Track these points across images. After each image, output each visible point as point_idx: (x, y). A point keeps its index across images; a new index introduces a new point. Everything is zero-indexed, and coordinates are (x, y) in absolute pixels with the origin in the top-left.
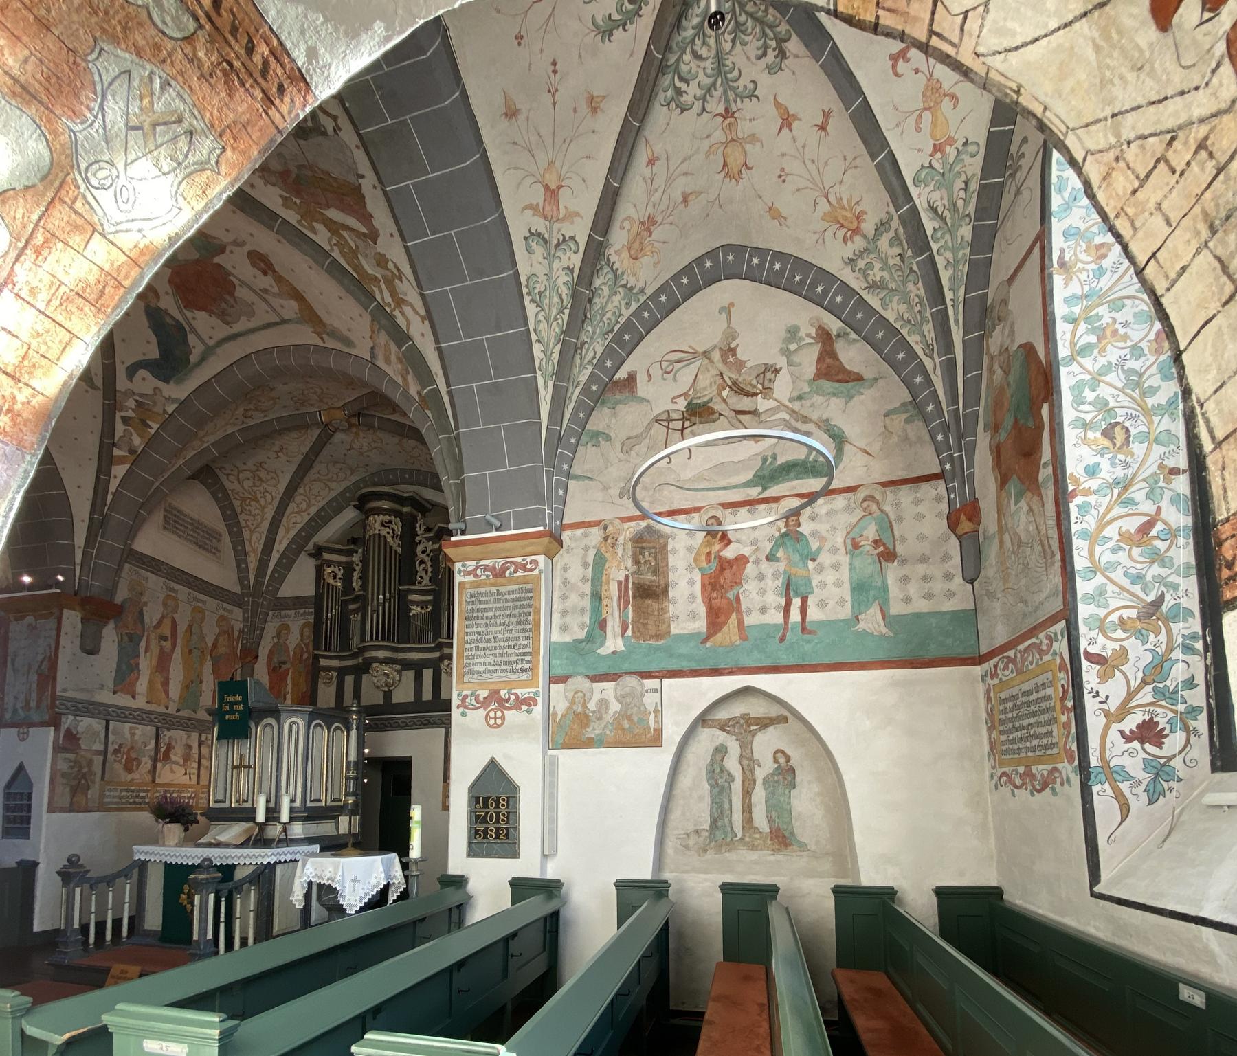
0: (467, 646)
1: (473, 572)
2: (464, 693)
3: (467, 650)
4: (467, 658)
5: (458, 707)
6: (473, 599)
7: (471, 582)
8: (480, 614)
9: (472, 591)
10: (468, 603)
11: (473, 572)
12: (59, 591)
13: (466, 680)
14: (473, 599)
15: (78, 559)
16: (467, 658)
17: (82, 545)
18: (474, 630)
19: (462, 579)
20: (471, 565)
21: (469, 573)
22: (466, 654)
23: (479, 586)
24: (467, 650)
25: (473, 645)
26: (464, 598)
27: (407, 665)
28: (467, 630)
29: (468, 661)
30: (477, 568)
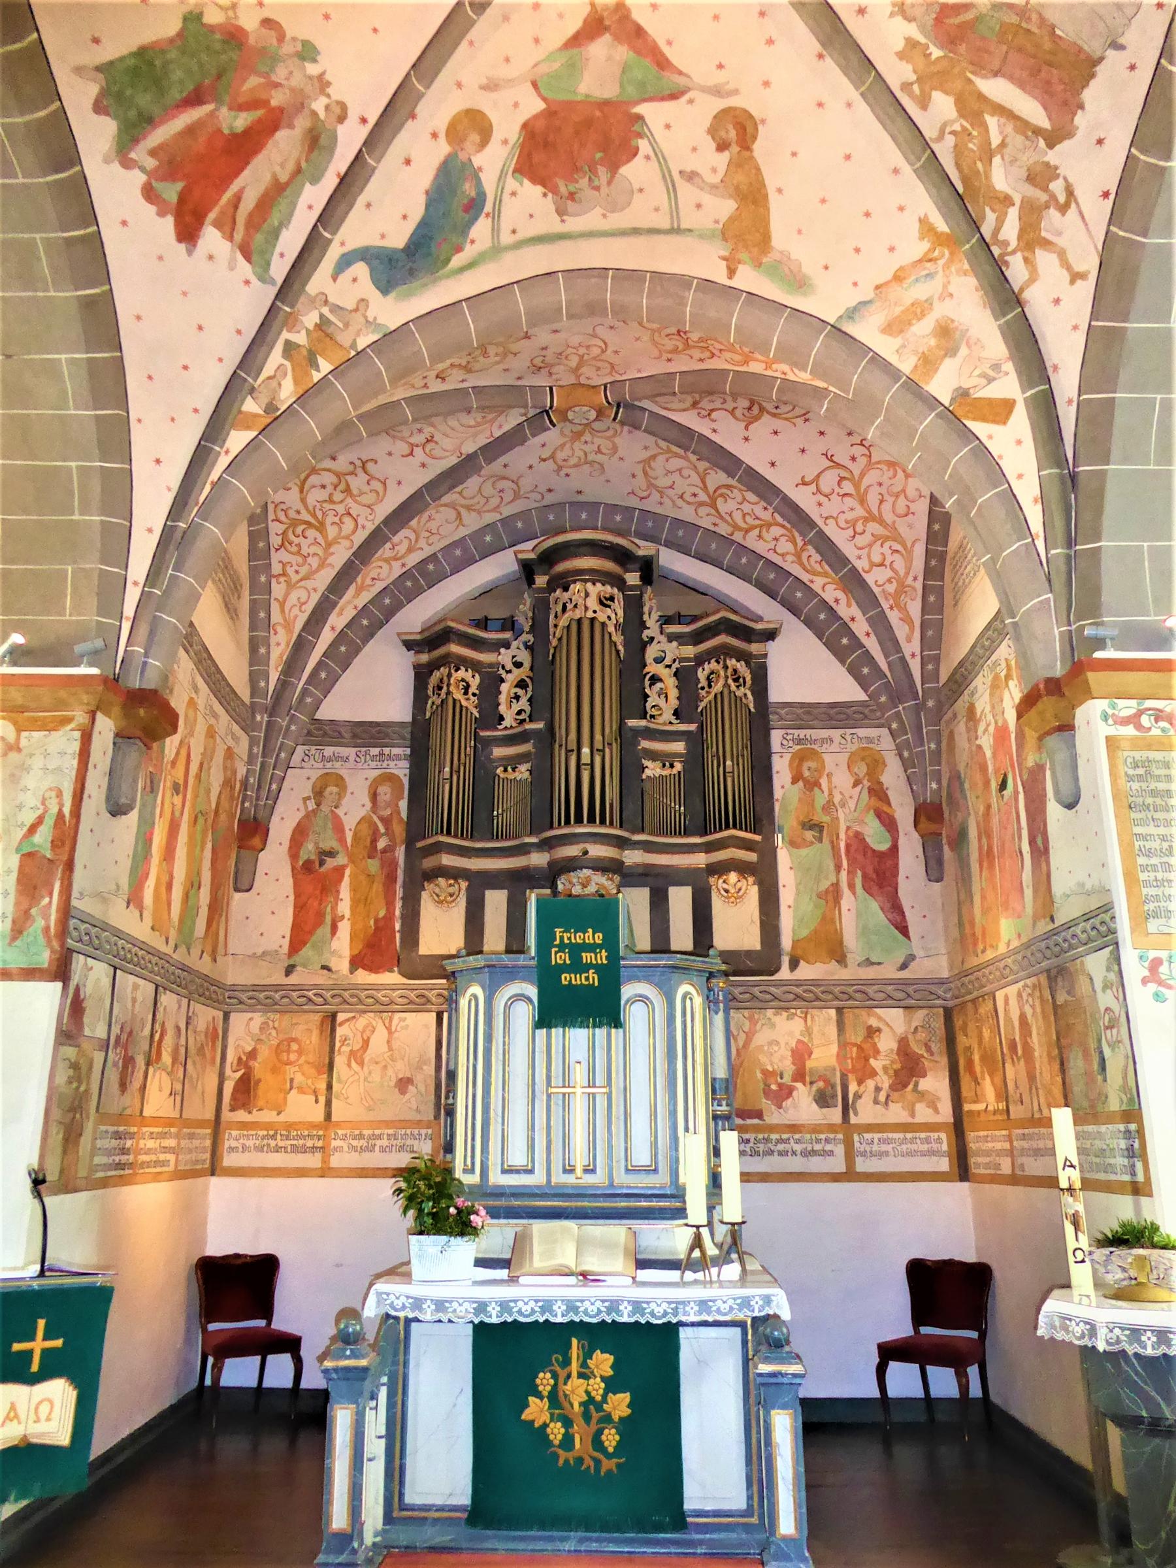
0: (1141, 860)
1: (1134, 720)
2: (1152, 954)
3: (1144, 868)
4: (1147, 883)
5: (1145, 981)
6: (1141, 771)
7: (1124, 738)
8: (1158, 801)
9: (1137, 755)
10: (1130, 778)
11: (1134, 720)
12: (95, 671)
13: (1153, 926)
14: (1141, 771)
15: (129, 609)
16: (1147, 883)
17: (142, 581)
18: (1151, 830)
19: (1113, 731)
20: (1127, 707)
21: (1125, 721)
22: (1143, 876)
23: (1149, 747)
24: (1144, 868)
25: (1154, 861)
26: (1122, 769)
27: (630, 877)
28: (1137, 830)
29: (1152, 891)
30: (1140, 713)
